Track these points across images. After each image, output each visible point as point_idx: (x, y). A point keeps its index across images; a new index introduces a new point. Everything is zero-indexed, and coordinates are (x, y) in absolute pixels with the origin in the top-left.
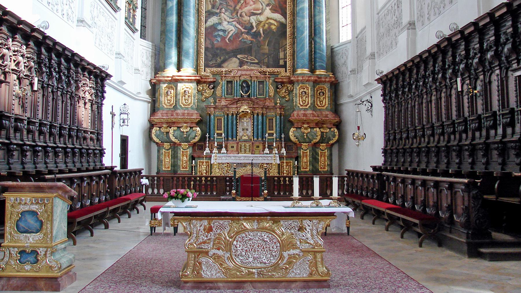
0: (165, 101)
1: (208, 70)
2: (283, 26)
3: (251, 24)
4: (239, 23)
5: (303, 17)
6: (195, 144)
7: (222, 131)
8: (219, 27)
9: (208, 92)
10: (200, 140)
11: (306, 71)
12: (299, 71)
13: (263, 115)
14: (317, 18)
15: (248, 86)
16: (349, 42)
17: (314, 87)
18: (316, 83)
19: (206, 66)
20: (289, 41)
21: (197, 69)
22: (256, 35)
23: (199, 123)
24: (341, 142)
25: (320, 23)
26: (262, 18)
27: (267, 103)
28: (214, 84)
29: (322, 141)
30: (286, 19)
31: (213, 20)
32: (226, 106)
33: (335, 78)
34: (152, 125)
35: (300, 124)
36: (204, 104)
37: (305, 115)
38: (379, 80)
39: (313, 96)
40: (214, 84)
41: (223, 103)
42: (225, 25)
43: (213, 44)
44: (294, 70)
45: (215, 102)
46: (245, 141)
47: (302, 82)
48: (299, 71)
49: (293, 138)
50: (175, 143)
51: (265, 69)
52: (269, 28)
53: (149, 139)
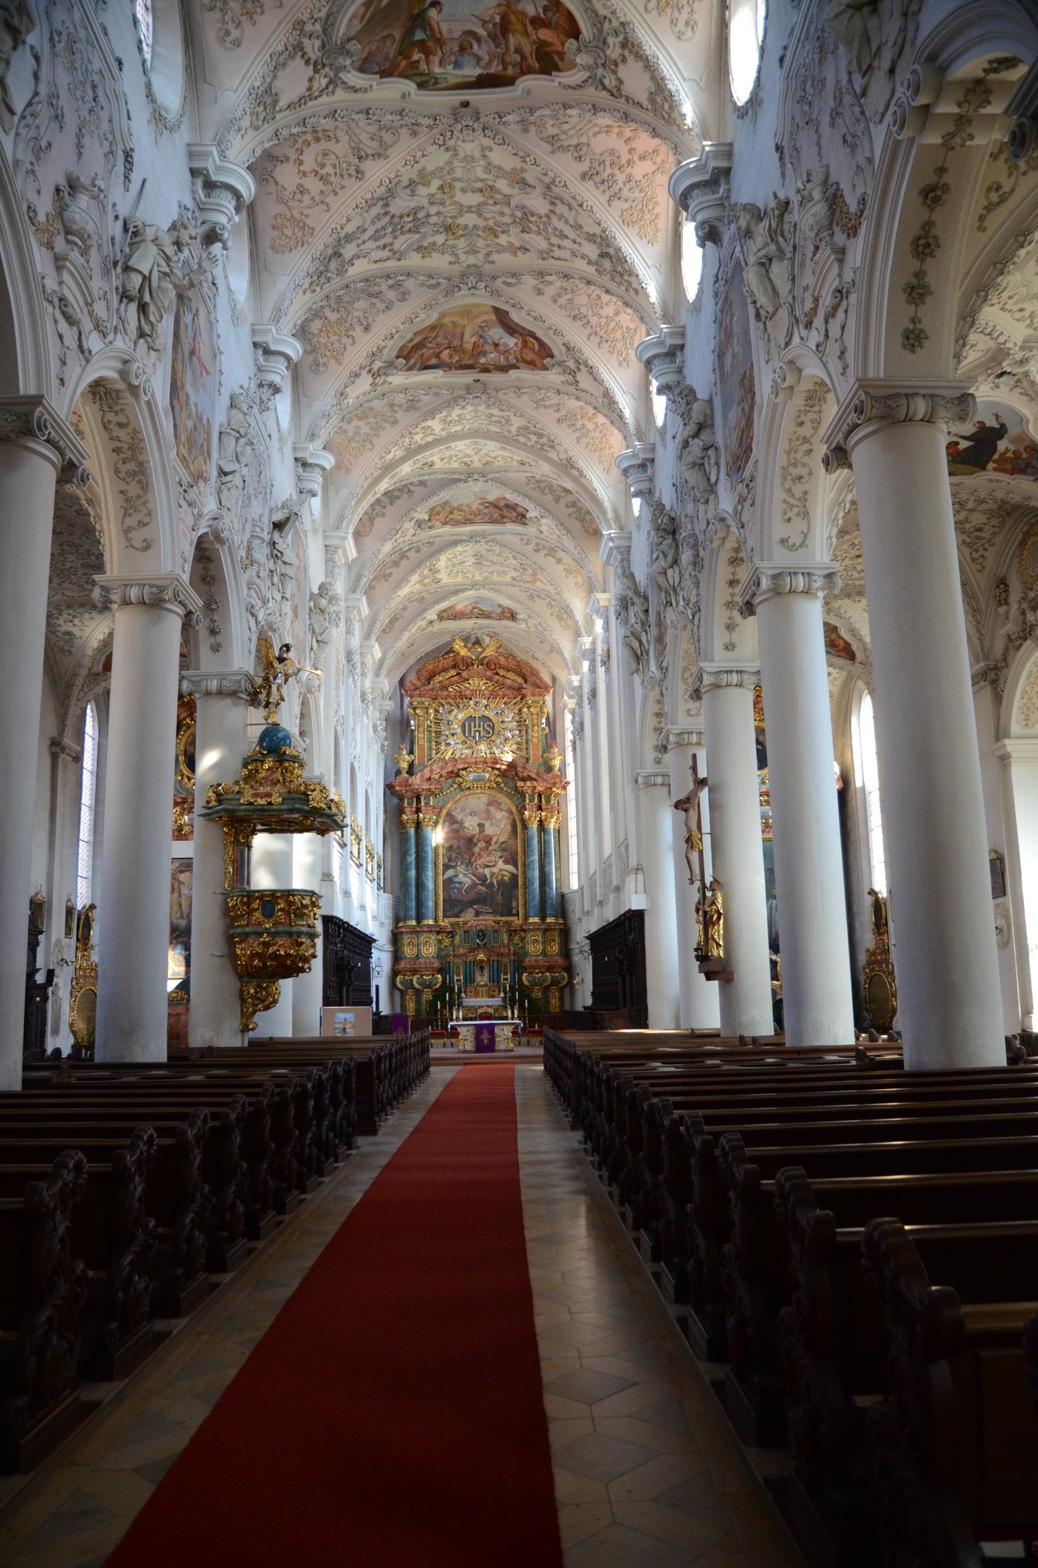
0: (408, 951)
1: (446, 920)
2: (514, 877)
3: (485, 876)
4: (474, 875)
5: (534, 870)
6: (436, 990)
7: (462, 977)
8: (456, 880)
9: (447, 942)
10: (441, 987)
11: (536, 920)
12: (531, 920)
13: (498, 961)
14: (547, 869)
15: (484, 935)
16: (576, 891)
17: (544, 934)
18: (545, 931)
19: (445, 916)
20: (520, 891)
21: (436, 920)
22: (492, 884)
23: (440, 971)
24: (570, 985)
25: (550, 874)
26: (495, 870)
27: (502, 951)
28: (452, 934)
29: (553, 983)
30: (517, 869)
31: (450, 873)
32: (464, 954)
33: (566, 924)
34: (395, 973)
35: (530, 971)
36: (444, 953)
37: (536, 961)
38: (588, 938)
39: (544, 943)
40: (452, 934)
41: (461, 951)
42: (461, 877)
43: (450, 895)
44: (526, 917)
45: (454, 951)
46: (482, 986)
47: (534, 930)
48: (531, 920)
49: (526, 983)
50: (418, 990)
51: (499, 918)
52: (502, 879)
53: (393, 985)
